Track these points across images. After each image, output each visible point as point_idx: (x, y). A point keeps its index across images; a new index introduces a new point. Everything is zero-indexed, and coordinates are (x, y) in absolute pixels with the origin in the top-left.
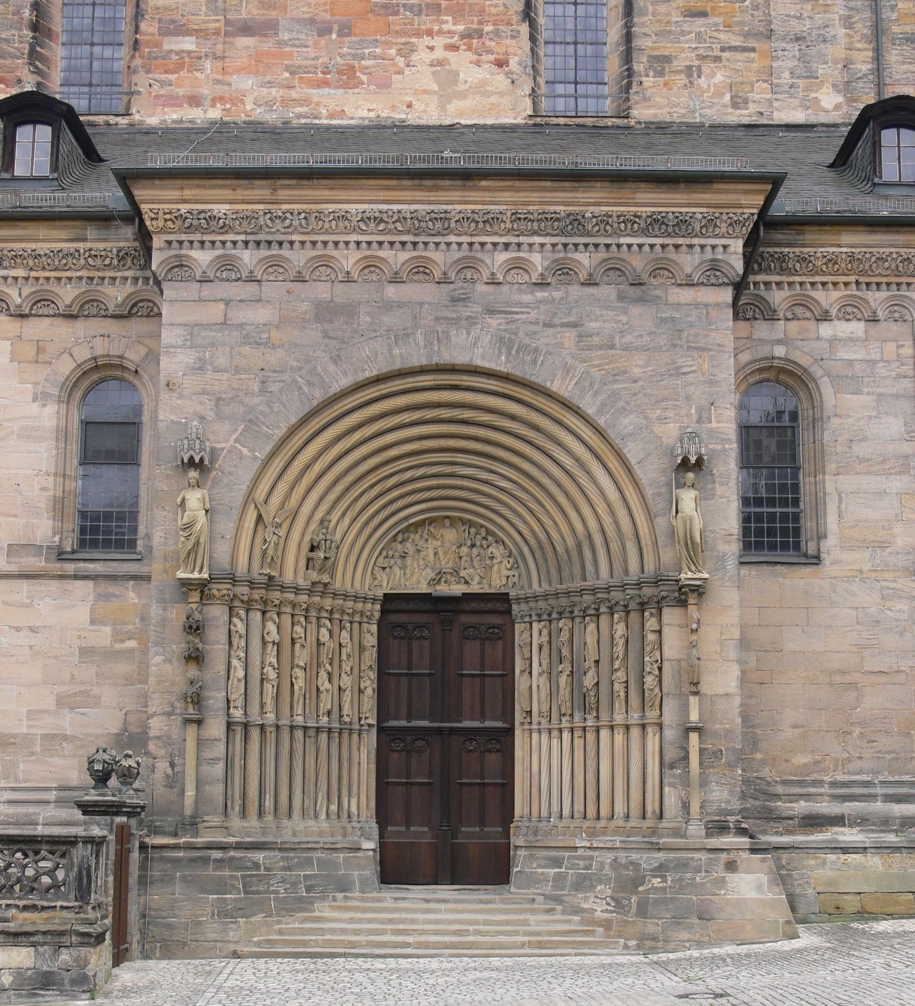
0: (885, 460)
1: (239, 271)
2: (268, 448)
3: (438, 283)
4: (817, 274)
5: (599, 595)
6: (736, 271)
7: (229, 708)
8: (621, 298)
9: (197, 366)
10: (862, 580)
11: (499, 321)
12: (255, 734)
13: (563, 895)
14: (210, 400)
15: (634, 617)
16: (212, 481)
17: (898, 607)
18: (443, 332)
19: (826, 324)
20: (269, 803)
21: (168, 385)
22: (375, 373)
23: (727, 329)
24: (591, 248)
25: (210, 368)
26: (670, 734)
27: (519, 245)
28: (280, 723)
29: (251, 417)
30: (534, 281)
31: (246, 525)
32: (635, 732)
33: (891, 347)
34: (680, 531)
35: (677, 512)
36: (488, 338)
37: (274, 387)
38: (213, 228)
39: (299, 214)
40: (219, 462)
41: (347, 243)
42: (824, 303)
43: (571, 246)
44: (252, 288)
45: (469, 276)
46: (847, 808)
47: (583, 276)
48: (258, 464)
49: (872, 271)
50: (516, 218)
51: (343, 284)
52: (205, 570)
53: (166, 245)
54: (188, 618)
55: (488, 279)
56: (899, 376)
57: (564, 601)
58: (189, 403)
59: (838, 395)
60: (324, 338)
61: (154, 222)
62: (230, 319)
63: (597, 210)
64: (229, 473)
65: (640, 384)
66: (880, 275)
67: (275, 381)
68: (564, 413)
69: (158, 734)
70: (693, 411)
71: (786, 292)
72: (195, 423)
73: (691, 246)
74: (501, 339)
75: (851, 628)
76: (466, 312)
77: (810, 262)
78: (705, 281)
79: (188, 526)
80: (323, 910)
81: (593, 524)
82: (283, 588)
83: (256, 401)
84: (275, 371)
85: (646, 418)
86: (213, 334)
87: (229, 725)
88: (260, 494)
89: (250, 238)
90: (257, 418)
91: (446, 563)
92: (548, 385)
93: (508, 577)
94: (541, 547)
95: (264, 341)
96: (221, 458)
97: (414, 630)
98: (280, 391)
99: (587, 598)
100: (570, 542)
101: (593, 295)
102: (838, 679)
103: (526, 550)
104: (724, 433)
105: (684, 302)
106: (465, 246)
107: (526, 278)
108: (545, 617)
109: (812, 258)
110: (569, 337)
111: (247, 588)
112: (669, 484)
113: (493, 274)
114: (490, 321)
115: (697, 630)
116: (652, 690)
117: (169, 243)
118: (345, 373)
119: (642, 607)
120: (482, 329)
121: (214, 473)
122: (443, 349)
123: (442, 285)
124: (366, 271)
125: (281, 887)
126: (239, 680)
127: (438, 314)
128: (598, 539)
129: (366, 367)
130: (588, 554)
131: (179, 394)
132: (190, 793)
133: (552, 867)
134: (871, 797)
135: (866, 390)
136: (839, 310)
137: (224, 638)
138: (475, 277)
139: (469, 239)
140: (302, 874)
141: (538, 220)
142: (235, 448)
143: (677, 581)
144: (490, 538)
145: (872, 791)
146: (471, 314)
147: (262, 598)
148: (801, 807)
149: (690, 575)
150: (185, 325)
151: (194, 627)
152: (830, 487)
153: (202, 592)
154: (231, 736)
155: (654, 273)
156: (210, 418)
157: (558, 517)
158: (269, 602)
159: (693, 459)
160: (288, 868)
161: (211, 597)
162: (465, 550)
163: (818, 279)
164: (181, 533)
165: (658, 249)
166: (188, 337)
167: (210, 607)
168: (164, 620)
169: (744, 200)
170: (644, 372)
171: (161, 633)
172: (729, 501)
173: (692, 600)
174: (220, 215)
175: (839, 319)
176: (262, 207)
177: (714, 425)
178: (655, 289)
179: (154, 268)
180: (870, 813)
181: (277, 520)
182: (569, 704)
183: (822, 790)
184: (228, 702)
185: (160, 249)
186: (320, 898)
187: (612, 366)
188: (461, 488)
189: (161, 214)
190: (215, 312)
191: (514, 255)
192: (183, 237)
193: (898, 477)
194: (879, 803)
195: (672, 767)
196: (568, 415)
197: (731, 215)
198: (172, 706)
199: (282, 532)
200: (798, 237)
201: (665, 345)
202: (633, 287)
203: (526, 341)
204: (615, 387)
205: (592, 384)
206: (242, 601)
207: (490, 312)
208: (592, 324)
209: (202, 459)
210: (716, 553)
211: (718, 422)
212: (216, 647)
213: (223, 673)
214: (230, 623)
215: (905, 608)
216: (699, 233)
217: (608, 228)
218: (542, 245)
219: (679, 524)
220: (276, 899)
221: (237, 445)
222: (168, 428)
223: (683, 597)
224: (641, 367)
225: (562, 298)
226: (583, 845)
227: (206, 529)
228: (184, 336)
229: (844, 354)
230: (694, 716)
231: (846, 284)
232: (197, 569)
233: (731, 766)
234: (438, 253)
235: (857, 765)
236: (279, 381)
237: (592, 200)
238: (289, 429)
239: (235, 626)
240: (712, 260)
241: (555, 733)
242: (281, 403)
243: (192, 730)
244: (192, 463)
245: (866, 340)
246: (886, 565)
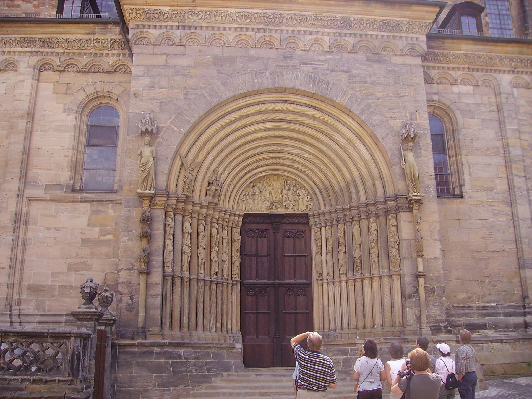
0: (488, 149)
1: (174, 40)
2: (188, 127)
3: (277, 49)
4: (450, 63)
5: (361, 209)
6: (423, 49)
7: (164, 267)
8: (368, 60)
9: (151, 85)
10: (483, 206)
11: (308, 68)
12: (178, 282)
13: (350, 370)
14: (157, 103)
15: (382, 218)
17: (501, 219)
18: (280, 72)
19: (455, 86)
20: (185, 321)
21: (135, 95)
22: (245, 91)
23: (421, 76)
24: (353, 35)
25: (157, 86)
26: (408, 279)
27: (317, 32)
28: (191, 277)
30: (325, 50)
31: (175, 168)
32: (386, 280)
33: (485, 98)
34: (408, 172)
35: (405, 163)
36: (303, 76)
37: (192, 97)
38: (161, 19)
39: (206, 12)
40: (162, 134)
41: (230, 28)
42: (454, 76)
43: (343, 34)
44: (180, 49)
45: (292, 46)
46: (487, 320)
47: (350, 48)
48: (182, 135)
49: (475, 63)
50: (316, 18)
51: (228, 48)
52: (152, 189)
53: (137, 27)
55: (302, 47)
56: (491, 111)
57: (340, 214)
59: (464, 119)
60: (218, 73)
61: (131, 15)
62: (169, 63)
63: (356, 17)
64: (167, 139)
65: (380, 101)
66: (478, 65)
67: (192, 94)
68: (342, 115)
69: (123, 281)
70: (408, 114)
71: (436, 71)
73: (401, 37)
74: (310, 76)
75: (480, 229)
76: (291, 63)
77: (448, 57)
78: (409, 54)
79: (145, 165)
80: (217, 382)
81: (356, 174)
82: (194, 204)
83: (181, 103)
84: (192, 89)
85: (385, 117)
86: (160, 70)
87: (164, 276)
88: (184, 151)
89: (180, 24)
90: (182, 112)
91: (276, 198)
92: (335, 99)
93: (307, 205)
94: (326, 188)
95: (186, 74)
96: (163, 132)
97: (259, 232)
99: (355, 211)
100: (343, 184)
101: (354, 58)
102: (476, 254)
103: (317, 191)
104: (424, 126)
105: (399, 63)
106: (290, 32)
107: (321, 48)
108: (329, 224)
109: (449, 55)
110: (344, 77)
112: (399, 150)
113: (305, 45)
114: (304, 68)
115: (420, 223)
116: (395, 256)
117: (138, 26)
118: (229, 91)
119: (387, 213)
120: (300, 72)
121: (158, 139)
122: (280, 81)
123: (279, 50)
124: (240, 42)
125: (193, 369)
126: (170, 252)
127: (277, 64)
128: (359, 181)
129: (240, 88)
130: (353, 190)
132: (142, 314)
133: (342, 355)
134: (497, 314)
135: (476, 117)
136: (461, 81)
137: (162, 227)
138: (295, 47)
139: (292, 29)
140: (205, 361)
141: (327, 20)
142: (170, 127)
143: (406, 198)
144: (297, 186)
145: (498, 311)
146: (294, 64)
148: (464, 320)
149: (415, 194)
150: (145, 66)
151: (146, 219)
152: (464, 161)
153: (150, 201)
154: (165, 283)
155: (384, 49)
157: (336, 172)
158: (186, 211)
159: (412, 136)
160: (197, 358)
161: (155, 204)
162: (285, 192)
163: (451, 65)
164: (140, 168)
165: (385, 37)
166: (146, 71)
169: (427, 16)
170: (382, 95)
172: (429, 159)
173: (416, 207)
174: (165, 12)
175: (461, 84)
176: (187, 8)
177: (419, 121)
178: (385, 57)
179: (129, 37)
180: (498, 323)
182: (344, 268)
183: (473, 311)
184: (164, 263)
185: (133, 28)
186: (214, 375)
187: (366, 91)
188: (284, 159)
189: (134, 10)
190: (161, 60)
191: (315, 36)
192: (146, 23)
193: (495, 157)
194: (501, 317)
195: (409, 297)
196: (344, 116)
197: (420, 23)
198: (132, 265)
199: (194, 174)
200: (442, 45)
201: (391, 82)
202: (374, 55)
203: (323, 78)
204: (368, 101)
205: (357, 100)
207: (304, 64)
208: (355, 71)
209: (152, 130)
210: (424, 185)
211: (421, 120)
212: (157, 232)
213: (161, 246)
214: (165, 220)
215: (504, 219)
216: (405, 31)
217: (361, 26)
218: (329, 33)
219: (407, 168)
220: (191, 376)
221: (171, 125)
223: (411, 206)
224: (380, 92)
225: (339, 59)
226: (360, 342)
227: (153, 168)
228: (144, 71)
229: (465, 100)
230: (421, 269)
231: (463, 69)
232: (148, 188)
233: (440, 296)
234: (277, 34)
235: (488, 298)
236: (195, 94)
237: (354, 12)
238: (199, 118)
240: (412, 44)
241: (337, 284)
243: (143, 278)
244: (146, 132)
245: (474, 95)
246: (493, 199)
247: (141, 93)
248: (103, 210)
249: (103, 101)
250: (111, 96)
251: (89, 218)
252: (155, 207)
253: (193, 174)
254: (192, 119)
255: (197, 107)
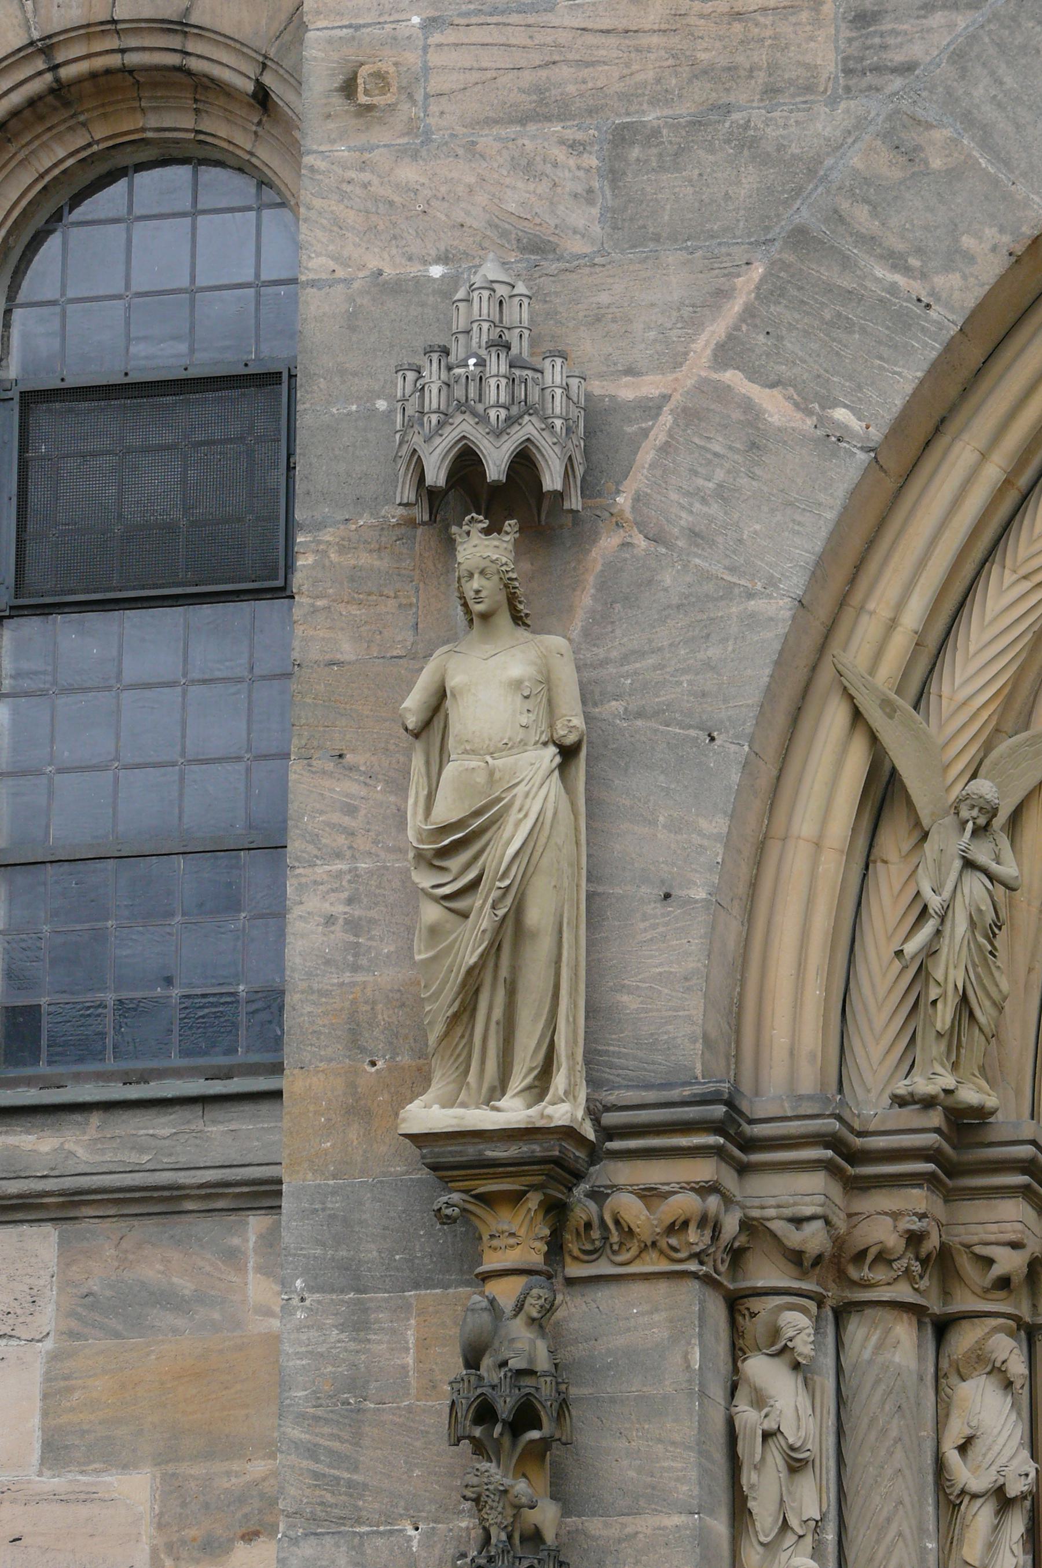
14: (575, 147)
16: (602, 586)
21: (349, 88)
29: (805, 215)
31: (805, 825)
40: (636, 482)
54: (473, 1358)
58: (464, 173)
64: (694, 534)
72: (491, 270)
90: (838, 218)
96: (646, 455)
98: (958, 57)
111: (816, 1182)
121: (608, 543)
131: (411, 129)
142: (723, 393)
147: (914, 1239)
156: (576, 246)
164: (425, 880)
167: (605, 1297)
168: (356, 1384)
171: (337, 1459)
181: (984, 787)
206: (796, 1258)
212: (644, 1524)
221: (731, 377)
222: (352, 321)
232: (519, 1080)
238: (1018, 261)
239: (760, 1401)
242: (968, 120)
247: (412, 58)
248: (185, 1285)
249: (128, 124)
250: (194, 64)
251: (48, 1378)
252: (604, 1267)
253: (1008, 869)
254: (939, 281)
255: (986, 143)
